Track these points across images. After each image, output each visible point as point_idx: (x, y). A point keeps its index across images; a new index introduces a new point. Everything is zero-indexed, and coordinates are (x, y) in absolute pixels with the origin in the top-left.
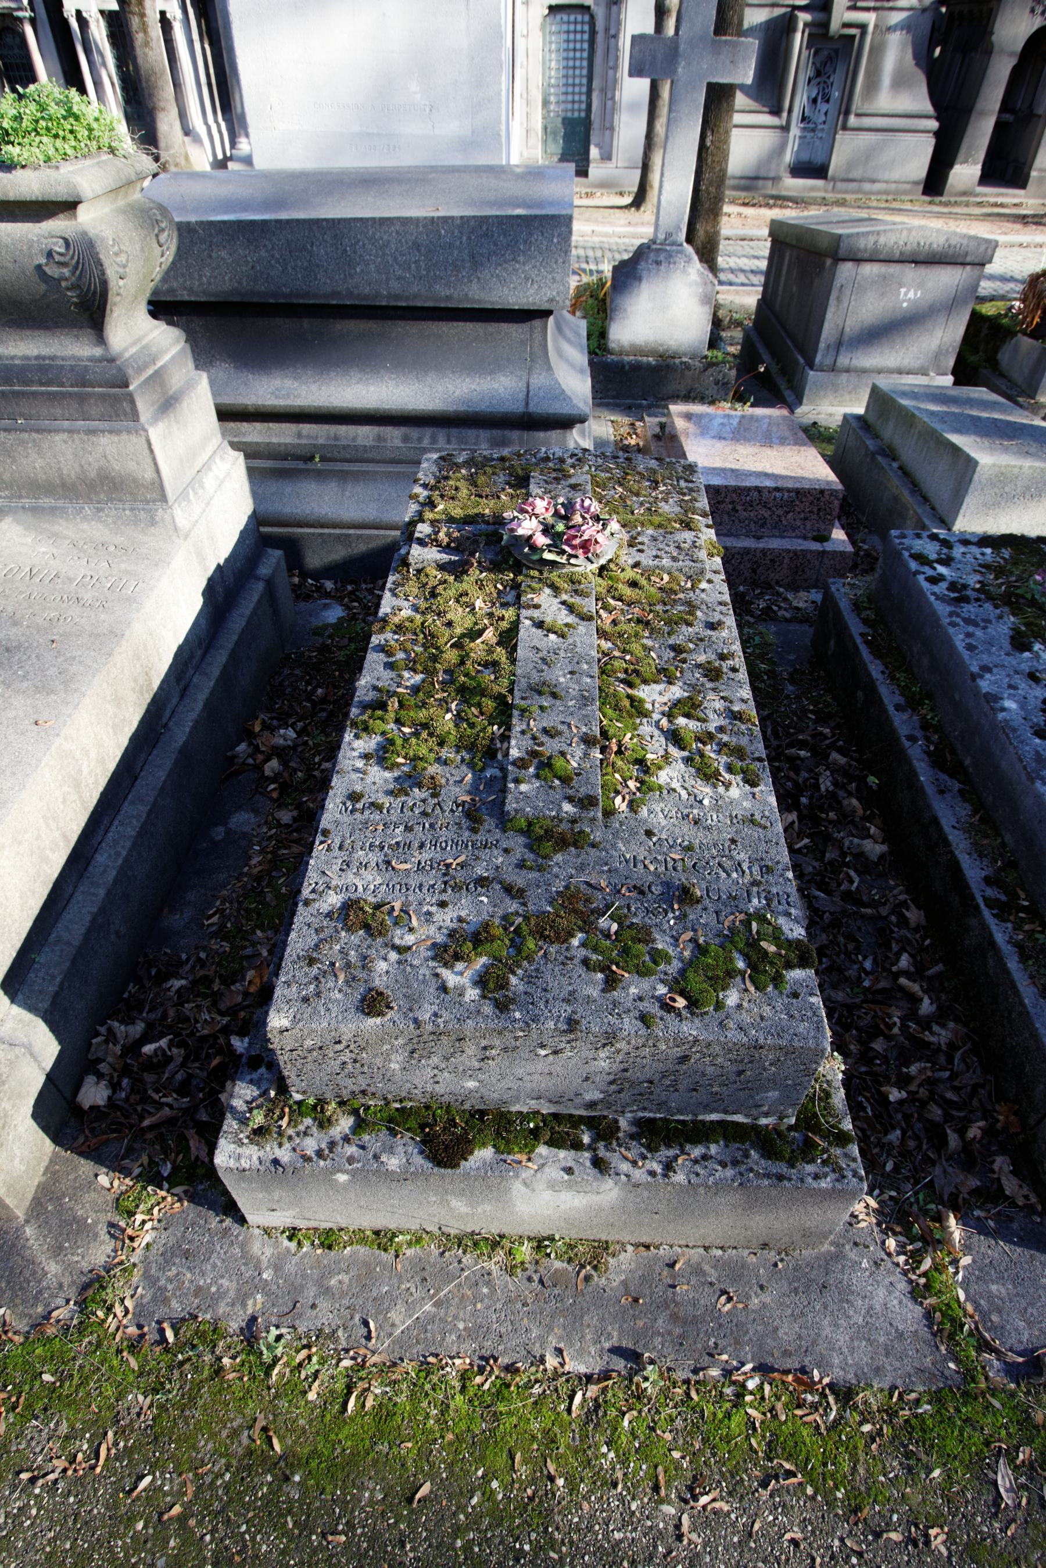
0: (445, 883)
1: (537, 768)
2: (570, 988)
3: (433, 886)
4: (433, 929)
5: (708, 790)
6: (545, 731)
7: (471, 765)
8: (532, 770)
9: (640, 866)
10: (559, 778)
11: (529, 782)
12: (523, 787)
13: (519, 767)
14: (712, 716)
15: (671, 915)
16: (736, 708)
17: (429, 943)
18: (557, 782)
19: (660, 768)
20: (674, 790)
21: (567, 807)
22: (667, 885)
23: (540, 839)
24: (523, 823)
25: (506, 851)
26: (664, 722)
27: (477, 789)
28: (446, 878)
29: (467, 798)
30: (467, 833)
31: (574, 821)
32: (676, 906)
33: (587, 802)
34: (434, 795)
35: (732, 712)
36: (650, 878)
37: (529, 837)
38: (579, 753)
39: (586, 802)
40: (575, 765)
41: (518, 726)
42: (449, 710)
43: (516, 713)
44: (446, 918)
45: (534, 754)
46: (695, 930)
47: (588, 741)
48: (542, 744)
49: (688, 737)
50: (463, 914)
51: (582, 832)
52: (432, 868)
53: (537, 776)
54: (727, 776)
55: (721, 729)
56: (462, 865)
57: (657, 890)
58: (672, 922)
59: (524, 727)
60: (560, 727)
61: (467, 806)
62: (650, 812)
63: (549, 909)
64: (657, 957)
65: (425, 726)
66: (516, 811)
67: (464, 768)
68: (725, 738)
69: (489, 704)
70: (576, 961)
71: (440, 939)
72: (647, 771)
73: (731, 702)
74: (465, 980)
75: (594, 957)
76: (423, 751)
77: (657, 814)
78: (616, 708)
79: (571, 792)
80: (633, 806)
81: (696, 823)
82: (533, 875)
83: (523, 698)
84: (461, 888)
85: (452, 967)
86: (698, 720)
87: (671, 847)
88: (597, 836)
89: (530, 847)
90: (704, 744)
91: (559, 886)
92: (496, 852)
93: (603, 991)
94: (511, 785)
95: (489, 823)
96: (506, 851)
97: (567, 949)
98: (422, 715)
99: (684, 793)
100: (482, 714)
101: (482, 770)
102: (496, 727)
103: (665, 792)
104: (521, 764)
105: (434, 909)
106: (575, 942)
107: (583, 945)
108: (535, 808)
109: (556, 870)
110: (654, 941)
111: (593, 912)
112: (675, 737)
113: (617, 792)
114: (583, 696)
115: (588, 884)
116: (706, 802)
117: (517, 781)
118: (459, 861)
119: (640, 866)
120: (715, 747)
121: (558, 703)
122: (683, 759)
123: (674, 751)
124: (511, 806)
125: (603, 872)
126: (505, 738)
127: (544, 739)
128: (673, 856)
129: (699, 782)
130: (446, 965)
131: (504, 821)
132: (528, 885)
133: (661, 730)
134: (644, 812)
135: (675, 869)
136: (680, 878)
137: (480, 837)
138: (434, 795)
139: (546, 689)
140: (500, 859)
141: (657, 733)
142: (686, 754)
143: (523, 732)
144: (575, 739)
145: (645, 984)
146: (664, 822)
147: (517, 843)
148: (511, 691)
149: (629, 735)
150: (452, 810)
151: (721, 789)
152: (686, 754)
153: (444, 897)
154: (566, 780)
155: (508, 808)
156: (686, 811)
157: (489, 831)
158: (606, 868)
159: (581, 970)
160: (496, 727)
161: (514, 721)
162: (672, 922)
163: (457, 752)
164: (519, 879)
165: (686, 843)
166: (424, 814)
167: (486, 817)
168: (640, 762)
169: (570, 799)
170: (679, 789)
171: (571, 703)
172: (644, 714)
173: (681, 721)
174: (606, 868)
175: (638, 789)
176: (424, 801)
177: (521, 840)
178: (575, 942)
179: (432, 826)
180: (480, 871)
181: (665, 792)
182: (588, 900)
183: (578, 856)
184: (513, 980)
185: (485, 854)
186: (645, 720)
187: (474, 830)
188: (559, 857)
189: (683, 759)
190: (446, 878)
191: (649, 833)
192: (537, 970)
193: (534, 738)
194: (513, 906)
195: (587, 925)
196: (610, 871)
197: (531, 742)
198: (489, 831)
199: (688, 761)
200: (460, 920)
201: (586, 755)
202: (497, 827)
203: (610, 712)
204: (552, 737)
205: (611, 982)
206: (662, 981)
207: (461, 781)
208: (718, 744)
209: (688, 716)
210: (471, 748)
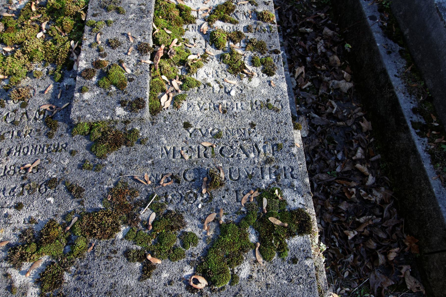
0: (23, 186)
1: (99, 77)
2: (112, 281)
3: (13, 189)
4: (9, 230)
5: (235, 82)
6: (108, 43)
7: (53, 77)
8: (94, 79)
9: (178, 156)
10: (115, 85)
11: (92, 90)
12: (87, 96)
13: (84, 78)
14: (242, 18)
15: (200, 199)
16: (260, 10)
17: (4, 244)
18: (114, 88)
19: (198, 67)
20: (209, 85)
21: (120, 111)
22: (198, 171)
23: (97, 141)
24: (87, 128)
25: (72, 153)
26: (205, 27)
27: (56, 97)
28: (24, 182)
29: (47, 107)
30: (44, 139)
31: (126, 122)
32: (204, 191)
33: (136, 105)
34: (23, 106)
35: (256, 13)
36: (186, 167)
37: (90, 140)
38: (133, 61)
39: (134, 105)
40: (129, 71)
41: (88, 39)
42: (41, 30)
43: (87, 28)
44: (19, 219)
45: (97, 64)
46: (218, 211)
47: (141, 49)
48: (105, 55)
49: (222, 38)
50: (33, 215)
51: (132, 130)
52: (15, 172)
53: (98, 85)
54: (250, 68)
55: (248, 29)
56: (38, 169)
57: (190, 177)
58: (200, 206)
59: (92, 41)
60: (122, 39)
61: (47, 113)
62: (189, 106)
63: (100, 206)
64: (188, 239)
65: (21, 44)
66: (79, 118)
67: (48, 79)
68: (250, 36)
69: (69, 22)
70: (120, 253)
71: (13, 240)
72: (188, 71)
73: (256, 5)
74: (28, 279)
75: (134, 247)
76: (17, 66)
77: (194, 108)
78: (168, 18)
79: (123, 97)
80: (176, 102)
81: (224, 112)
82: (91, 174)
83: (94, 15)
84: (34, 190)
85: (20, 267)
86: (231, 22)
87: (204, 135)
88: (145, 133)
89: (89, 148)
90: (234, 42)
91: (110, 183)
92: (64, 154)
93: (140, 279)
94: (77, 95)
95: (62, 127)
96: (72, 153)
97: (113, 243)
98: (18, 36)
99: (216, 86)
100: (64, 31)
101: (61, 80)
102: (72, 42)
103: (202, 87)
104: (87, 74)
105: (11, 211)
106: (120, 235)
107: (126, 237)
108: (93, 114)
109: (108, 168)
110: (184, 225)
111: (136, 204)
112: (212, 39)
113: (164, 91)
114: (141, 10)
115: (133, 178)
116: (233, 93)
117: (81, 91)
118: (35, 165)
119: (178, 156)
120: (243, 45)
121: (121, 17)
122: (217, 56)
123: (212, 52)
124: (75, 114)
125: (147, 165)
126: (78, 51)
127: (107, 50)
128: (205, 144)
129: (229, 76)
130: (14, 266)
131: (72, 127)
132: (86, 184)
133: (202, 33)
134: (184, 106)
135: (205, 155)
136: (208, 164)
137: (54, 141)
138: (23, 106)
139: (112, 5)
140: (67, 161)
141: (199, 36)
142: (220, 52)
143: (90, 46)
144: (132, 48)
145: (175, 267)
146: (199, 114)
147: (80, 144)
148: (85, 10)
149: (176, 40)
150: (35, 119)
151: (245, 80)
152: (220, 52)
153: (21, 200)
154: (120, 86)
155: (72, 116)
156: (217, 102)
157: (61, 135)
158: (150, 162)
159: (122, 262)
160: (72, 42)
161: (86, 36)
162: (200, 206)
163: (44, 66)
164: (78, 178)
165: (216, 131)
166: (14, 123)
167: (60, 123)
168: (183, 62)
169: (122, 103)
170: (212, 84)
171: (131, 17)
172: (189, 21)
173: (218, 24)
174: (150, 162)
175: (181, 87)
176: (15, 111)
177: (85, 142)
178: (120, 235)
179: (19, 133)
180: (51, 173)
181: (202, 87)
182: (133, 194)
183: (128, 153)
184: (67, 277)
185: (55, 157)
186: (190, 26)
187: (49, 135)
188: (112, 156)
189: (217, 56)
190: (25, 181)
191: (187, 126)
192: (86, 266)
193: (99, 50)
194: (72, 205)
195: (131, 219)
196: (153, 164)
197: (96, 54)
198: (61, 135)
199: (221, 58)
200: (31, 220)
201: (139, 61)
202: (67, 132)
203: (161, 21)
204: (113, 48)
205: (147, 270)
206: (189, 263)
207: (43, 92)
208: (245, 42)
209: (223, 19)
210: (54, 62)
